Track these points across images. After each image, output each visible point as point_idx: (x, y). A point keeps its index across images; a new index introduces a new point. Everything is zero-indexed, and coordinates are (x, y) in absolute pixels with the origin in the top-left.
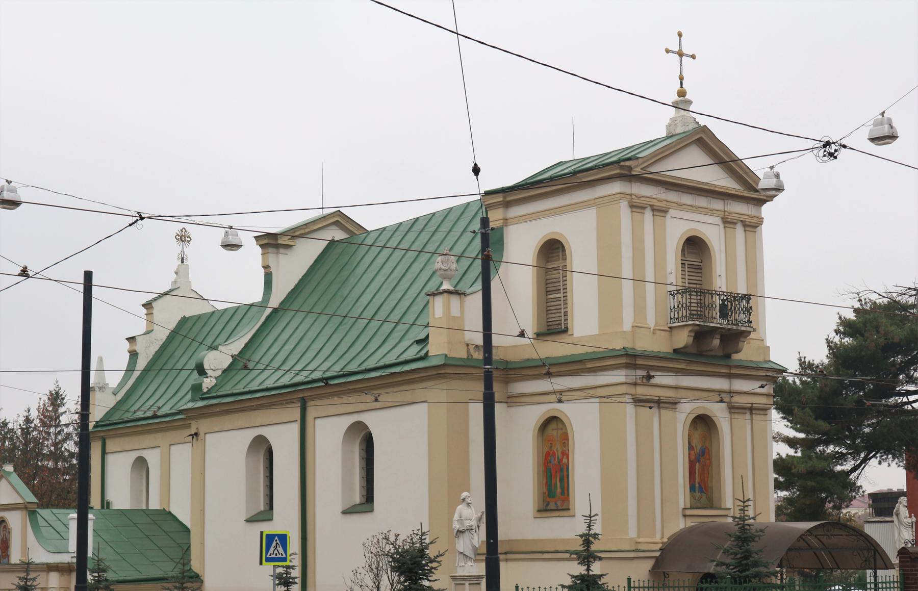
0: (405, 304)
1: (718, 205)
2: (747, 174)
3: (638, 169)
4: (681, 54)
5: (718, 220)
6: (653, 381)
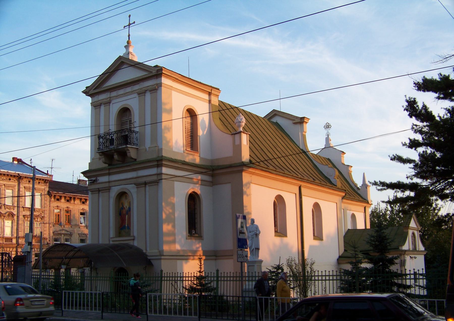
0: (271, 145)
1: (137, 87)
2: (144, 67)
3: (92, 90)
4: (129, 25)
5: (136, 95)
6: (98, 182)
